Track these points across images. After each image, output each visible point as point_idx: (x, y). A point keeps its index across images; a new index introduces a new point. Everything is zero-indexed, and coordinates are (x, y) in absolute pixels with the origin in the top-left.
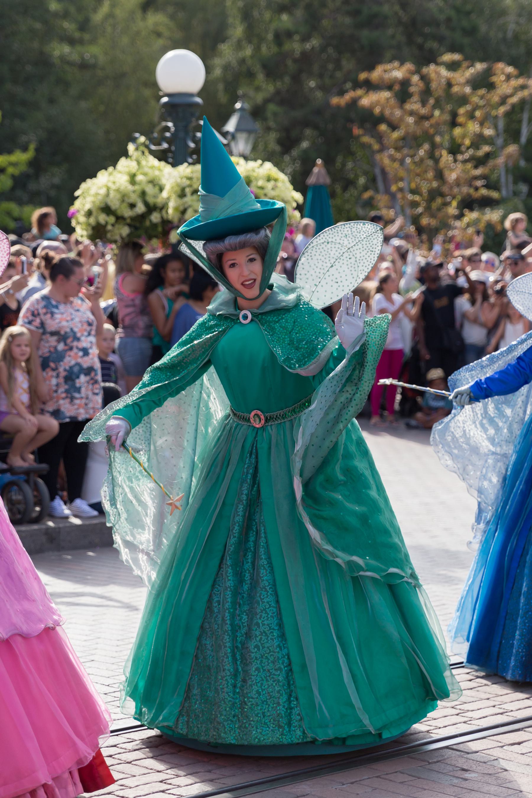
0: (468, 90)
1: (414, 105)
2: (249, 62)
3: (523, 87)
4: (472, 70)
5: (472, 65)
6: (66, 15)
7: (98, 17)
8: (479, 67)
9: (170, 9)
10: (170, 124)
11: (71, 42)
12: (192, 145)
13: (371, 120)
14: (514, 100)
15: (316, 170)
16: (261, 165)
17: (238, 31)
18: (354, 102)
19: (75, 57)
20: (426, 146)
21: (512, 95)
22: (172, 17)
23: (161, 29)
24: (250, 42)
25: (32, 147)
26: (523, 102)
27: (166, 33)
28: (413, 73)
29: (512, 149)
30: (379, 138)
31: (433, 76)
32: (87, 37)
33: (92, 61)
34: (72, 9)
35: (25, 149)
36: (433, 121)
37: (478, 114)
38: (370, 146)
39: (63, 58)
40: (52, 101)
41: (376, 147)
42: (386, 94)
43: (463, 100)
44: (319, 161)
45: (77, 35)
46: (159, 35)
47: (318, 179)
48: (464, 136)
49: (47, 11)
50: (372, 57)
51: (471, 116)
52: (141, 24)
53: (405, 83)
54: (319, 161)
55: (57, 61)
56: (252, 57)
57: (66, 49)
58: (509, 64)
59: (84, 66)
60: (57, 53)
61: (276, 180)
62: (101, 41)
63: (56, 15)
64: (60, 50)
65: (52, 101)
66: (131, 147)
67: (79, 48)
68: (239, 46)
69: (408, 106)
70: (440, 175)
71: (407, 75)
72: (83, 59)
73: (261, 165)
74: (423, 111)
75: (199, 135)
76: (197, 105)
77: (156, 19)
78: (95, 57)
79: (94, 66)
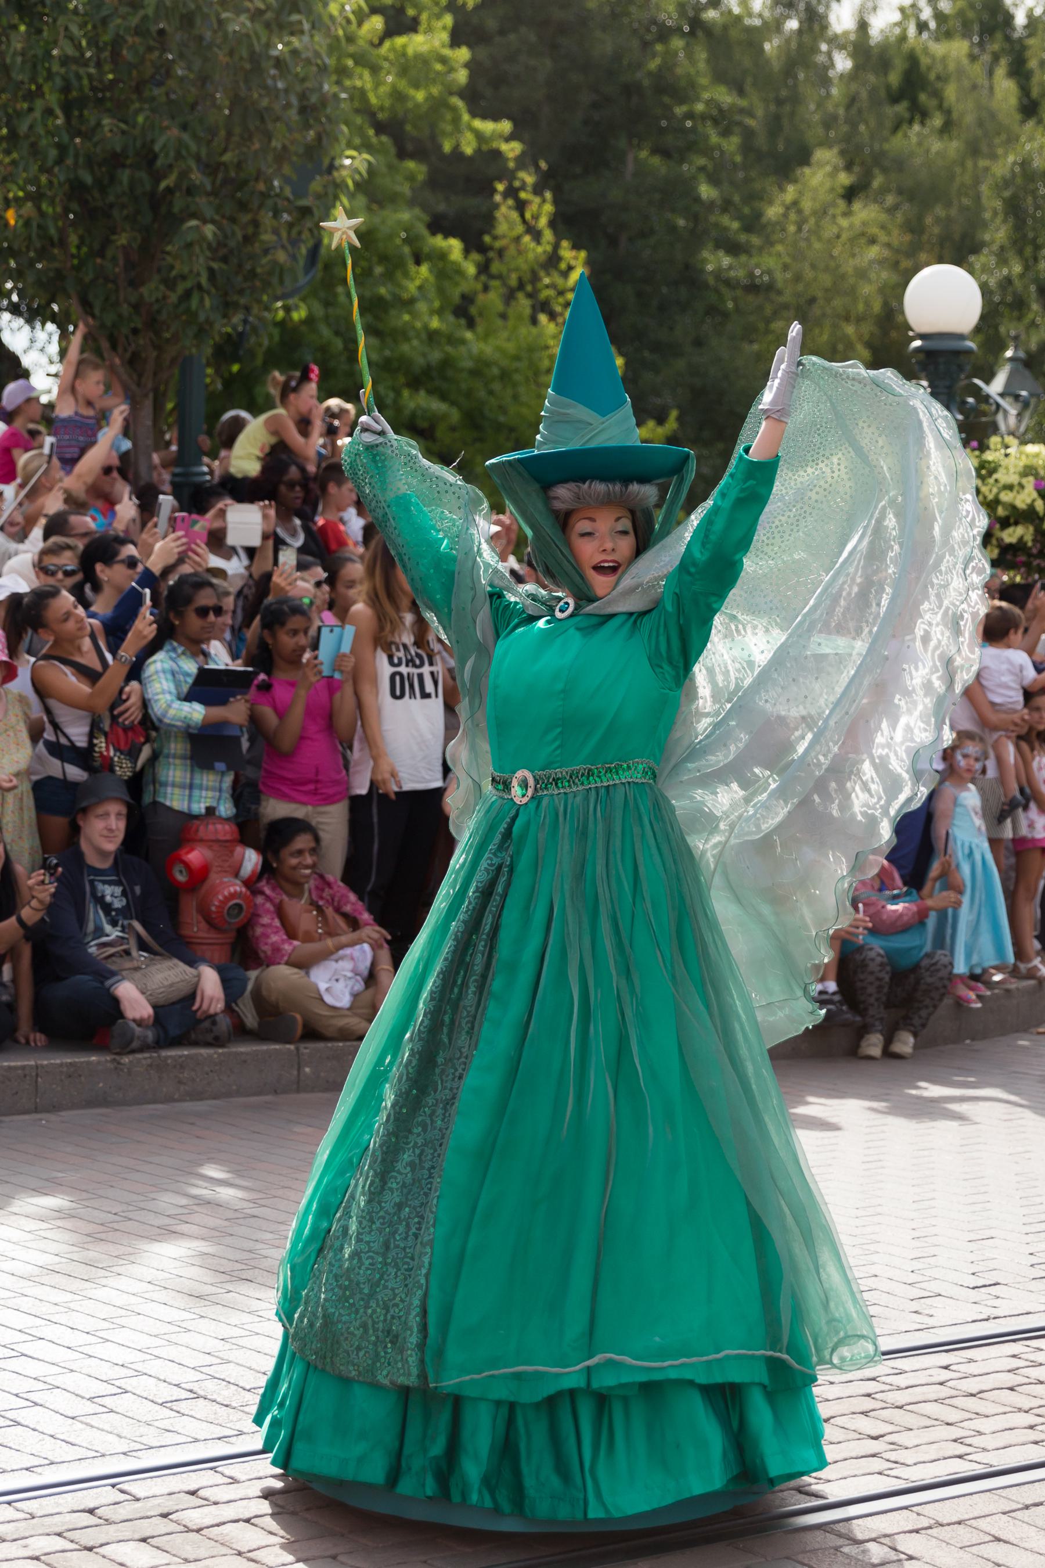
2: (1017, 283)
6: (727, 206)
7: (773, 212)
9: (890, 200)
11: (734, 248)
17: (998, 233)
19: (739, 274)
22: (892, 210)
23: (875, 230)
24: (1020, 252)
25: (674, 414)
27: (883, 238)
32: (755, 240)
33: (766, 278)
34: (737, 198)
35: (661, 421)
39: (718, 274)
40: (699, 343)
45: (743, 237)
46: (873, 241)
49: (697, 199)
52: (844, 223)
55: (711, 281)
56: (1022, 276)
57: (726, 261)
59: (753, 287)
60: (710, 267)
62: (779, 248)
63: (711, 205)
64: (715, 261)
65: (699, 343)
67: (743, 258)
68: (1002, 260)
72: (751, 275)
77: (865, 213)
78: (769, 272)
79: (770, 287)
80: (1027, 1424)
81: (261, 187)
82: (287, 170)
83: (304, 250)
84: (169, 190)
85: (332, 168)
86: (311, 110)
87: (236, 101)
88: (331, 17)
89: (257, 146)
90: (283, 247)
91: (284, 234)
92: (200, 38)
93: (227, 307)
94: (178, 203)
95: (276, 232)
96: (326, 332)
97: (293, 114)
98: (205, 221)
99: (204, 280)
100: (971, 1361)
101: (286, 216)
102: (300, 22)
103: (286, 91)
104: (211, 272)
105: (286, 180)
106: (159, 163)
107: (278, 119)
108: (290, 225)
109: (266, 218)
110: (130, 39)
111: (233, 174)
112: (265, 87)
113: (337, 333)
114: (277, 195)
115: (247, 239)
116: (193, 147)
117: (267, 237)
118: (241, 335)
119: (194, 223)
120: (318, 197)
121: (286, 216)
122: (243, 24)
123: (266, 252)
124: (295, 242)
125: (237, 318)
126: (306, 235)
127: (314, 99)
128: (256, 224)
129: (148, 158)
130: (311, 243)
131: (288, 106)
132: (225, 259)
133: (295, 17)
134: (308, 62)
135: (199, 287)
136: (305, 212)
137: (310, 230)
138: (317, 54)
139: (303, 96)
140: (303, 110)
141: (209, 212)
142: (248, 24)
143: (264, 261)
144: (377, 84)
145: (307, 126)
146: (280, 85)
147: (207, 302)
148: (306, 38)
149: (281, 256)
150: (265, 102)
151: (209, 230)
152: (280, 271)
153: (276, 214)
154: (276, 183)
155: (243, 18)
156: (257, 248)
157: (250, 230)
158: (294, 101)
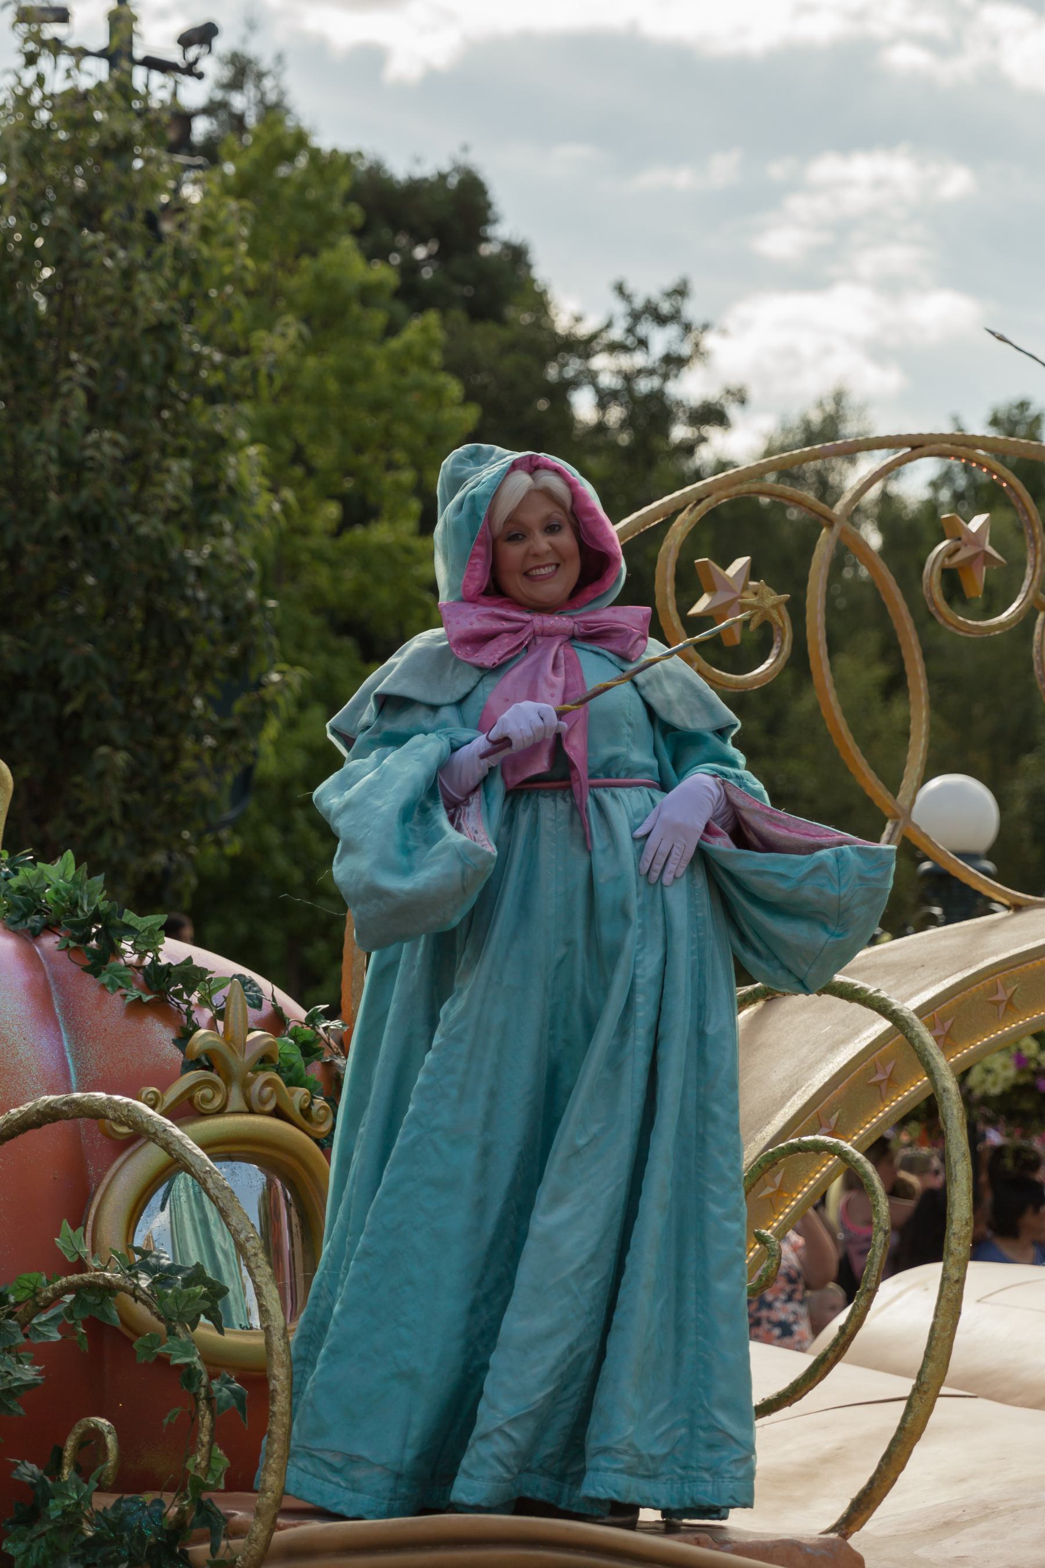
81: (181, 707)
82: (211, 689)
83: (229, 778)
84: (76, 715)
85: (259, 685)
86: (236, 621)
87: (151, 613)
88: (258, 517)
89: (175, 661)
90: (207, 775)
91: (207, 759)
92: (107, 545)
93: (144, 843)
94: (87, 730)
95: (197, 757)
96: (281, 862)
97: (216, 628)
98: (116, 748)
99: (116, 815)
101: (209, 741)
102: (221, 524)
103: (210, 601)
104: (125, 808)
105: (209, 700)
106: (65, 684)
107: (196, 631)
108: (214, 751)
109: (188, 744)
110: (29, 547)
111: (148, 694)
112: (184, 598)
113: (296, 863)
114: (200, 717)
115: (167, 767)
116: (103, 665)
117: (188, 764)
118: (166, 872)
119: (104, 750)
120: (246, 717)
121: (209, 741)
122: (155, 529)
123: (189, 777)
124: (220, 768)
125: (160, 858)
126: (231, 761)
127: (239, 606)
128: (177, 750)
129: (50, 678)
130: (237, 769)
131: (210, 617)
132: (142, 790)
133: (216, 518)
134: (230, 566)
135: (111, 823)
136: (231, 735)
137: (236, 755)
138: (241, 559)
139: (225, 607)
140: (226, 620)
141: (120, 738)
142: (161, 526)
143: (187, 788)
144: (336, 580)
145: (230, 638)
146: (201, 595)
147: (122, 840)
148: (227, 542)
149: (205, 786)
150: (184, 613)
151: (121, 758)
152: (202, 802)
153: (199, 738)
154: (199, 702)
155: (156, 522)
156: (177, 777)
157: (168, 757)
158: (217, 612)
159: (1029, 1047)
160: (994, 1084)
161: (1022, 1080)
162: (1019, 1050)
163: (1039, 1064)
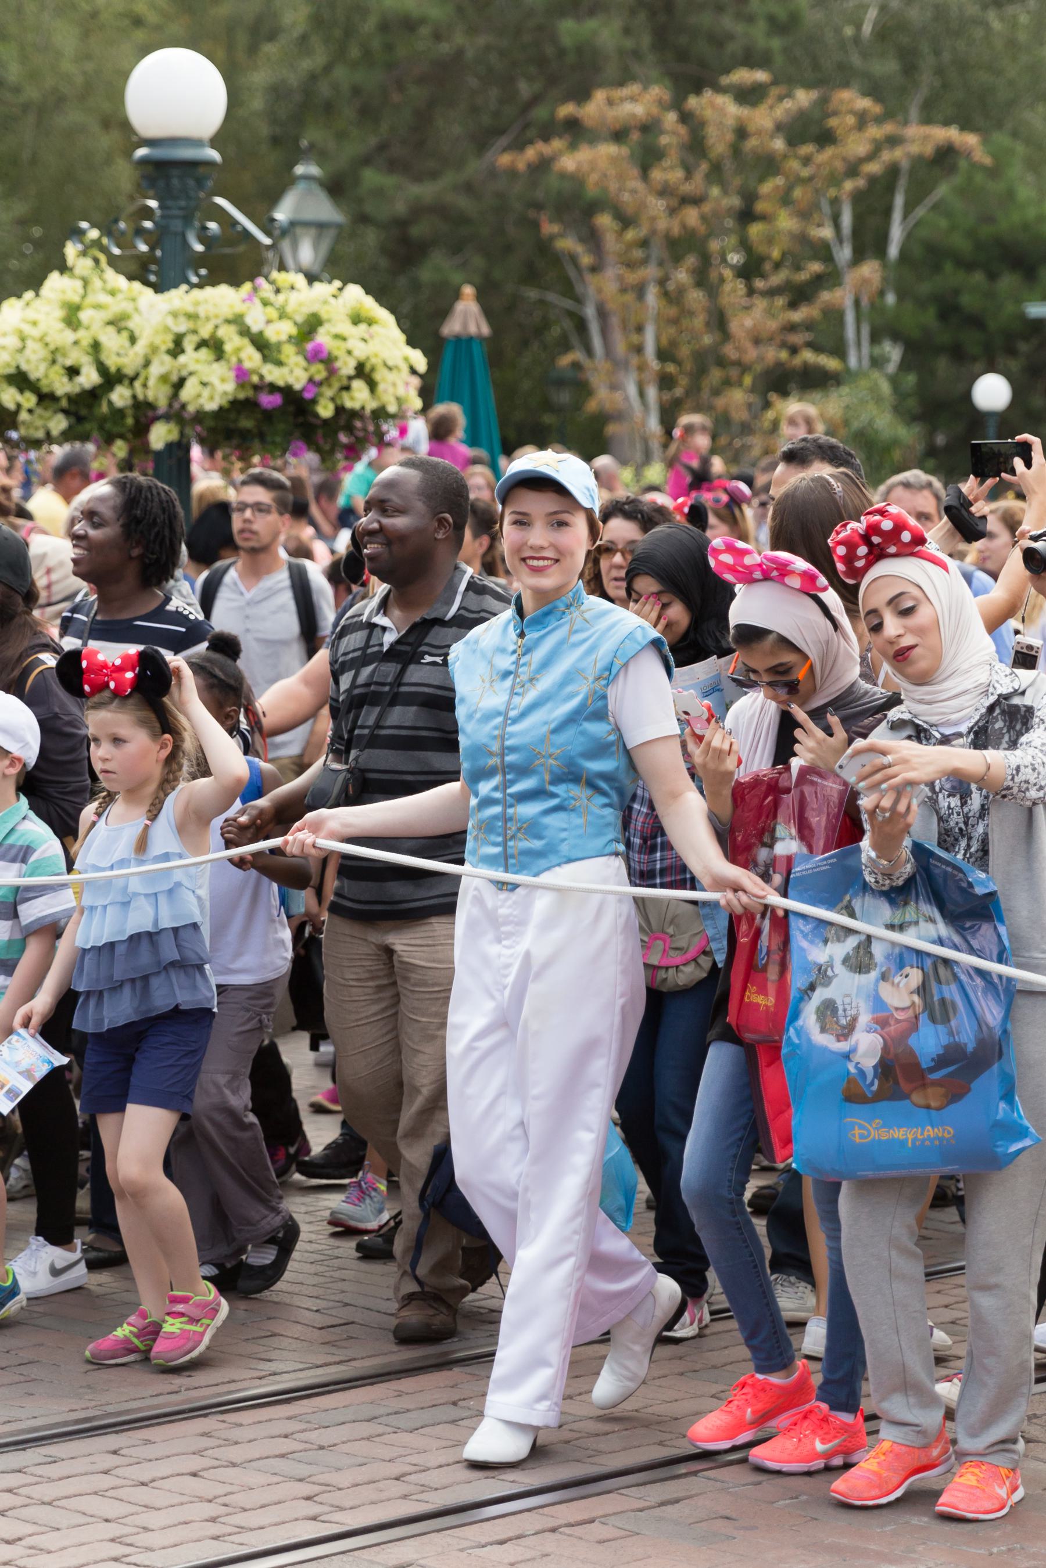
0: (779, 144)
1: (668, 173)
3: (893, 141)
4: (788, 104)
5: (789, 95)
8: (804, 98)
10: (153, 204)
12: (199, 248)
13: (580, 207)
14: (874, 168)
15: (460, 306)
16: (340, 289)
18: (543, 165)
20: (691, 260)
21: (871, 157)
26: (893, 171)
28: (664, 107)
29: (870, 270)
30: (593, 238)
31: (708, 113)
36: (707, 208)
37: (798, 193)
38: (573, 259)
41: (586, 260)
42: (608, 150)
43: (769, 165)
44: (468, 290)
47: (465, 325)
48: (770, 240)
50: (581, 75)
51: (785, 199)
53: (649, 128)
54: (468, 290)
58: (865, 94)
61: (371, 322)
66: (71, 250)
69: (657, 175)
70: (719, 321)
71: (655, 110)
73: (340, 289)
74: (687, 188)
75: (213, 226)
76: (210, 164)
80: (206, 1516)
100: (148, 1442)
159: (250, 358)
160: (212, 398)
161: (241, 396)
162: (240, 361)
163: (262, 377)
